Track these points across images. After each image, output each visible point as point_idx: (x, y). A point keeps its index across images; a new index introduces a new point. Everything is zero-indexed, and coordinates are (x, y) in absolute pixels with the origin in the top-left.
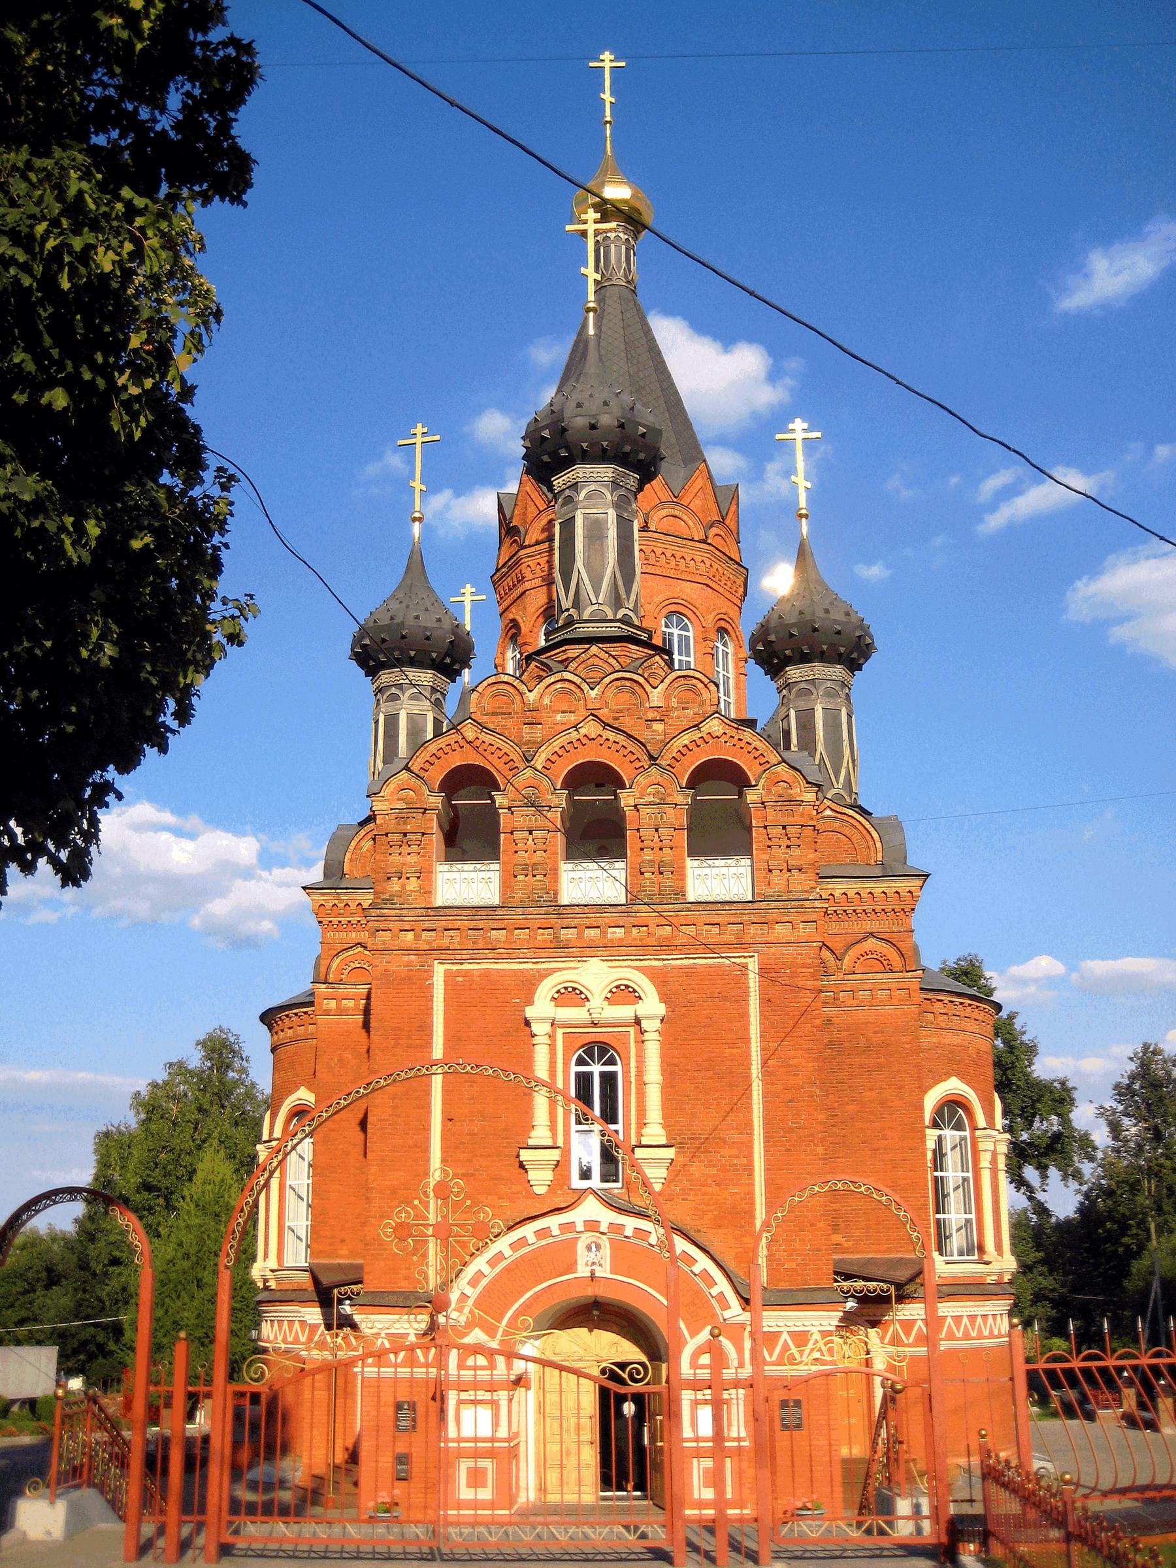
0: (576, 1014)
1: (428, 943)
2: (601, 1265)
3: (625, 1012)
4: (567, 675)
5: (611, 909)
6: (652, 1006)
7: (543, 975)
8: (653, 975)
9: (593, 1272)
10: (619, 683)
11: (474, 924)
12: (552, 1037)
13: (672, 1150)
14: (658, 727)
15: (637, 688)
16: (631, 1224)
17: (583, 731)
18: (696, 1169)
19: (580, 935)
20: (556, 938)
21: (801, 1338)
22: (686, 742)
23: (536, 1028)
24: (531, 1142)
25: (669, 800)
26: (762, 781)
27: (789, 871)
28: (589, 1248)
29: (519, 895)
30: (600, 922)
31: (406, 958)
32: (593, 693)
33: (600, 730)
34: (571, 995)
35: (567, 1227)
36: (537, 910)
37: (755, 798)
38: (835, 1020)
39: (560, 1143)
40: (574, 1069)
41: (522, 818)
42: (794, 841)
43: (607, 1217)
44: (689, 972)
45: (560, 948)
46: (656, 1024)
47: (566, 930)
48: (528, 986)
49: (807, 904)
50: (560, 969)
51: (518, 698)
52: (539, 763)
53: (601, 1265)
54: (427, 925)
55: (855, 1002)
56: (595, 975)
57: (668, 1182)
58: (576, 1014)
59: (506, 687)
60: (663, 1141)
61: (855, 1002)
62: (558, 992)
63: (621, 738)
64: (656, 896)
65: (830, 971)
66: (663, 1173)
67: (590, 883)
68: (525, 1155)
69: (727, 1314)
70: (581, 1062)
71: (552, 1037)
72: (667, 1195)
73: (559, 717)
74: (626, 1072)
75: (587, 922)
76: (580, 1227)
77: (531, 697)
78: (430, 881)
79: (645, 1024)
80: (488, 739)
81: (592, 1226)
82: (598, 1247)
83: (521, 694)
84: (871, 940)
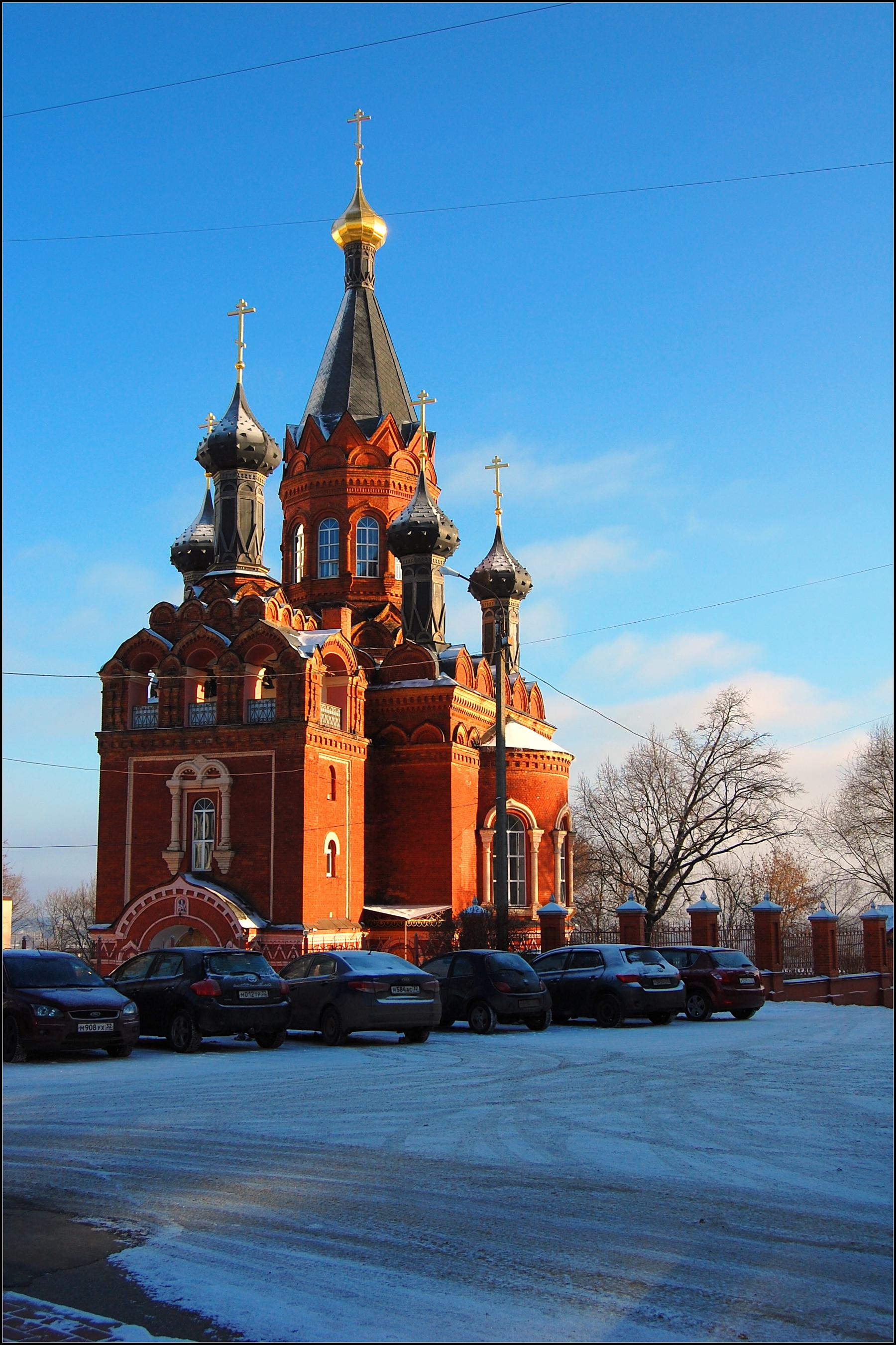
6: (225, 779)
7: (178, 762)
17: (198, 633)
23: (172, 792)
28: (180, 903)
34: (188, 775)
35: (169, 892)
48: (170, 767)
50: (184, 761)
56: (199, 764)
57: (231, 868)
66: (228, 865)
71: (181, 796)
76: (175, 893)
81: (180, 891)
82: (184, 902)
84: (427, 725)
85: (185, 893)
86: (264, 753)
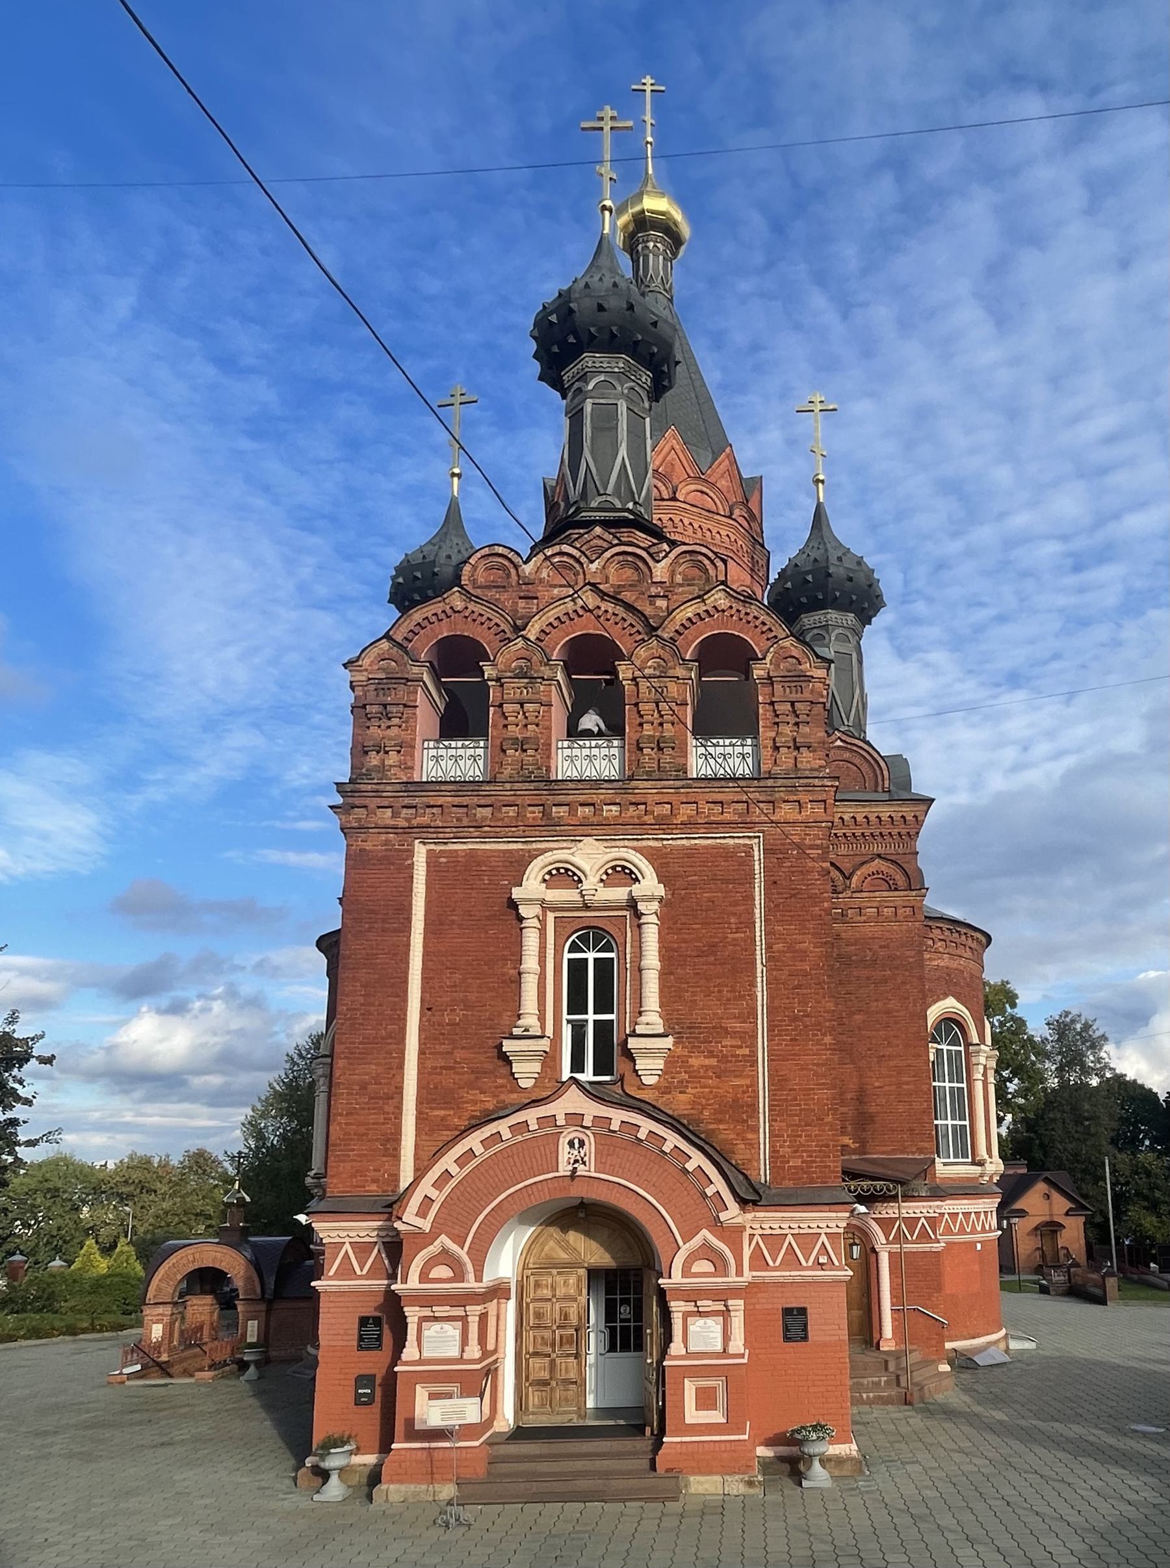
0: (569, 895)
1: (408, 820)
2: (584, 1163)
3: (619, 894)
4: (566, 548)
5: (606, 785)
6: (650, 885)
8: (651, 856)
9: (575, 1170)
10: (621, 558)
11: (457, 800)
12: (543, 922)
13: (670, 1039)
14: (662, 603)
15: (640, 564)
16: (618, 1117)
18: (695, 1062)
19: (572, 813)
20: (546, 814)
21: (807, 1240)
22: (690, 615)
23: (523, 911)
24: (516, 1031)
25: (671, 673)
26: (769, 656)
27: (798, 748)
28: (571, 1144)
29: (508, 771)
30: (595, 799)
31: (383, 837)
32: (593, 567)
33: (598, 602)
36: (527, 786)
37: (762, 673)
38: (843, 935)
39: (549, 1031)
40: (567, 956)
41: (515, 688)
42: (803, 718)
43: (591, 1109)
44: (690, 853)
45: (551, 827)
46: (655, 906)
47: (556, 808)
48: (517, 866)
49: (816, 782)
50: (551, 850)
51: (513, 571)
52: (532, 632)
53: (584, 1163)
54: (407, 801)
55: (863, 918)
56: (590, 856)
58: (569, 895)
59: (500, 560)
60: (661, 1031)
61: (863, 918)
62: (549, 873)
63: (620, 610)
64: (651, 766)
65: (840, 889)
67: (588, 760)
68: (508, 1046)
69: (723, 1216)
70: (574, 948)
72: (663, 1089)
73: (556, 591)
74: (622, 956)
75: (582, 798)
77: (528, 569)
78: (413, 756)
79: (641, 907)
80: (478, 609)
81: (575, 1119)
82: (582, 1144)
83: (516, 567)
85: (587, 1122)
86: (732, 840)
